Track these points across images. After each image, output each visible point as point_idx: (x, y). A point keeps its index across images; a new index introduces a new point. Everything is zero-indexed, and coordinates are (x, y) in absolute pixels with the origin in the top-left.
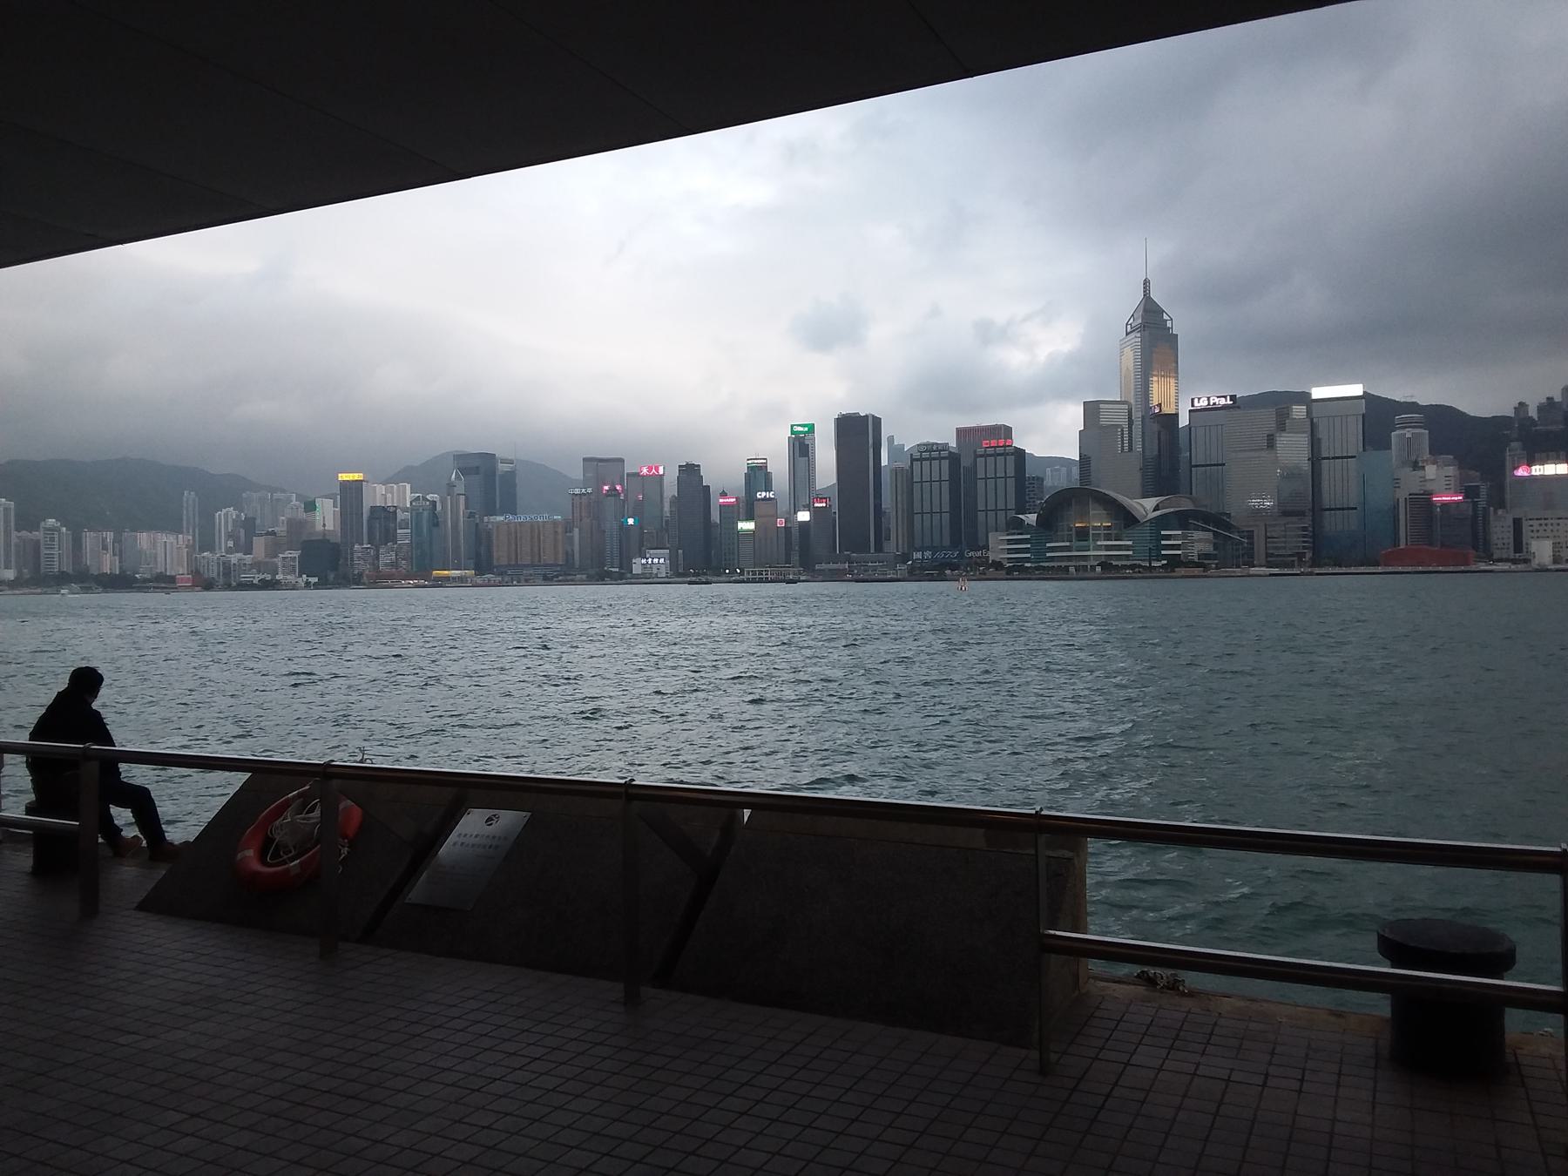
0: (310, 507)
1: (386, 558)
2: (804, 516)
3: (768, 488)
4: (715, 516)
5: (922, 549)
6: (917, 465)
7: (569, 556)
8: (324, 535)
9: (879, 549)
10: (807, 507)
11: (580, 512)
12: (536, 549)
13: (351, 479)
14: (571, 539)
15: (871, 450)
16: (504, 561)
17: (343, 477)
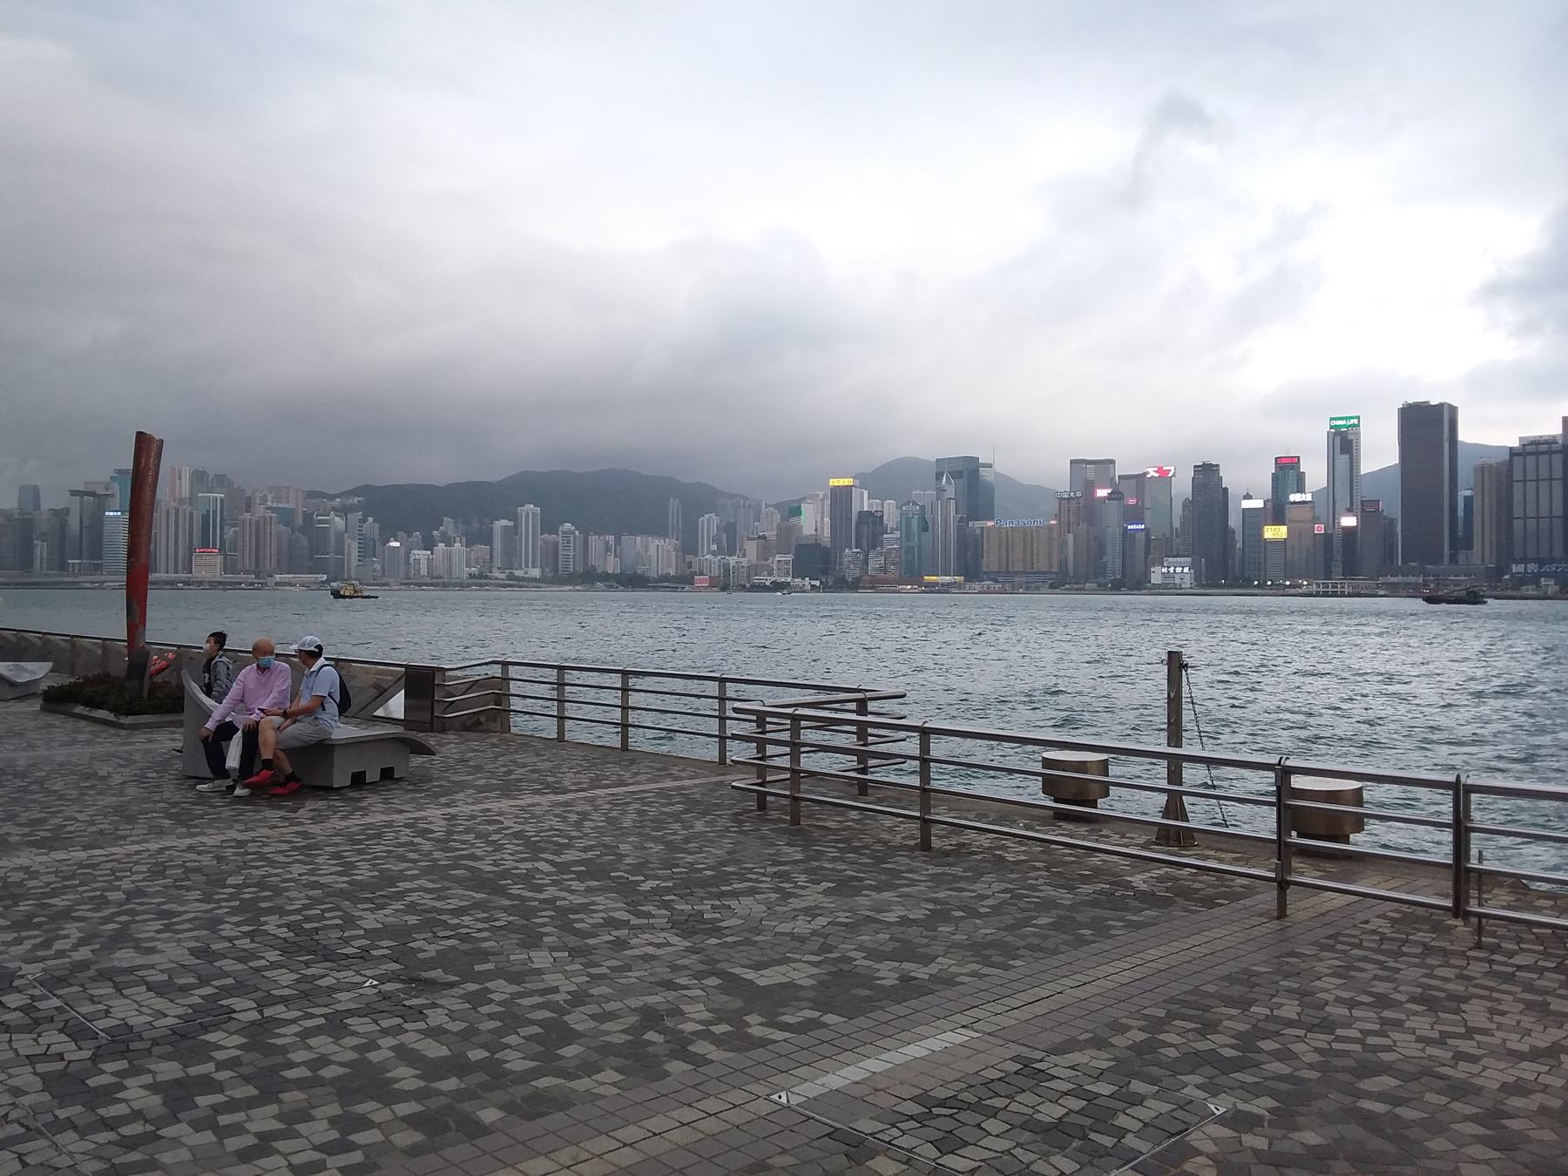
0: (796, 512)
1: (875, 563)
2: (1349, 521)
3: (1301, 490)
4: (1234, 521)
5: (1525, 560)
6: (1518, 461)
7: (1063, 563)
8: (816, 540)
9: (1453, 559)
10: (1350, 511)
11: (1068, 518)
12: (1029, 555)
13: (841, 484)
14: (1065, 543)
15: (1446, 445)
16: (994, 568)
17: (834, 482)
